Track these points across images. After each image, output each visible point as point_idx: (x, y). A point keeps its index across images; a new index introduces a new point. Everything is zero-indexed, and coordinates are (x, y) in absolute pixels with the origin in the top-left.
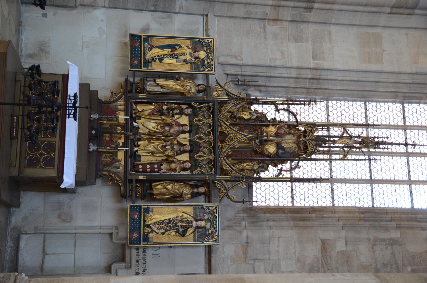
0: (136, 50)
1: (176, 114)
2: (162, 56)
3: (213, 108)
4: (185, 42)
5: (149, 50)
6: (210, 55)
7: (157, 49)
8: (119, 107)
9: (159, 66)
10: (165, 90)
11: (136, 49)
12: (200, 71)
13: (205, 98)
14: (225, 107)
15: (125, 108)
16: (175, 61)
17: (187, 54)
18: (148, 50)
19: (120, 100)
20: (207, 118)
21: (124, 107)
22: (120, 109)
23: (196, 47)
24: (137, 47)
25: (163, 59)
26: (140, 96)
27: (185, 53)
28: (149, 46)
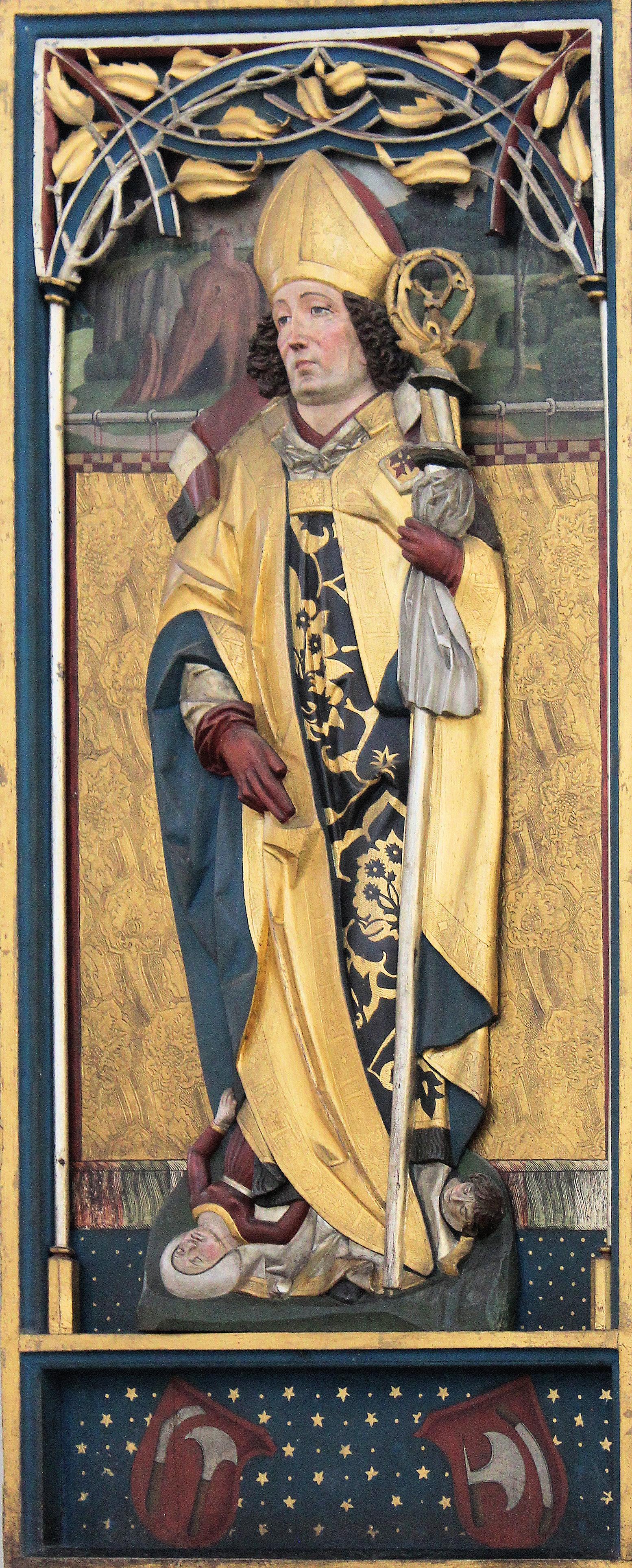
4: (115, 569)
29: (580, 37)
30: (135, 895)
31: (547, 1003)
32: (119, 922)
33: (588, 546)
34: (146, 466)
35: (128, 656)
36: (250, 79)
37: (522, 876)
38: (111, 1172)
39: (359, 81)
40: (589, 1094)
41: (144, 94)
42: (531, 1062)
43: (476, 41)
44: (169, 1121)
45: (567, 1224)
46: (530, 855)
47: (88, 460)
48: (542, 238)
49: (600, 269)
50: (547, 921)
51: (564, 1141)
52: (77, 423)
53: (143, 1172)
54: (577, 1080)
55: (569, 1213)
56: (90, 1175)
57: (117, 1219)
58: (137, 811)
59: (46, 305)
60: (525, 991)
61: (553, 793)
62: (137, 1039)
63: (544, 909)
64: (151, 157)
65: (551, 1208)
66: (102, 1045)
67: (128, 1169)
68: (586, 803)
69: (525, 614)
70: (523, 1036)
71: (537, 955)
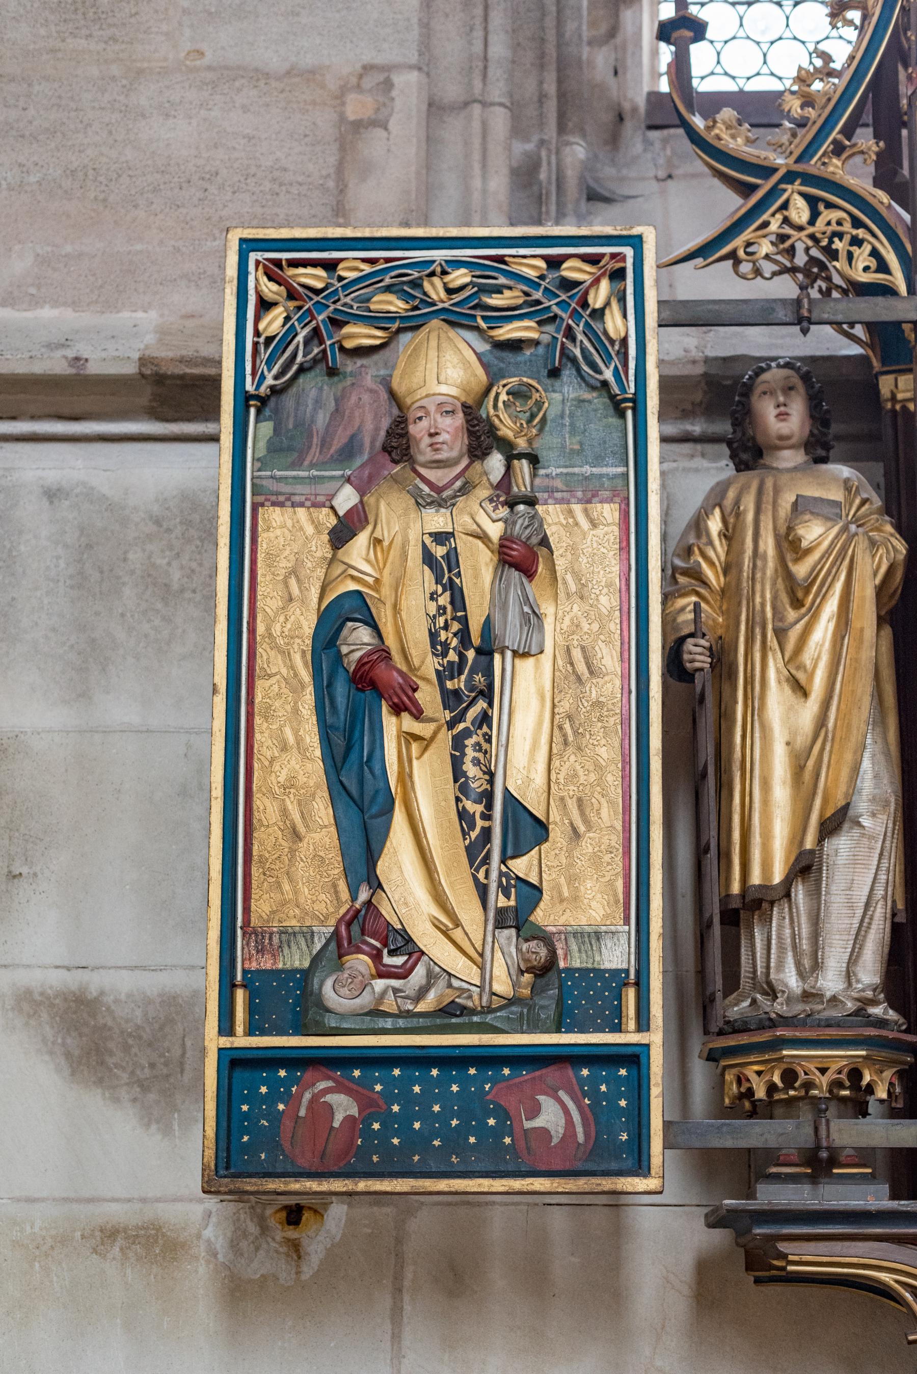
0: (406, 1118)
2: (471, 807)
4: (284, 564)
5: (399, 960)
6: (435, 290)
7: (382, 867)
9: (587, 846)
10: (867, 784)
11: (387, 1119)
12: (638, 403)
16: (526, 667)
17: (441, 538)
18: (404, 973)
23: (339, 440)
24: (367, 1104)
27: (428, 559)
28: (361, 962)
30: (293, 762)
31: (582, 828)
32: (282, 779)
33: (612, 553)
34: (308, 503)
35: (293, 617)
36: (392, 278)
37: (565, 751)
38: (271, 934)
39: (467, 279)
40: (612, 885)
41: (319, 285)
42: (571, 865)
44: (314, 902)
45: (596, 966)
46: (571, 738)
47: (267, 500)
49: (632, 390)
50: (582, 779)
51: (594, 914)
52: (259, 477)
53: (295, 934)
55: (597, 958)
56: (257, 935)
57: (275, 963)
58: (296, 711)
59: (248, 407)
60: (566, 822)
61: (588, 701)
62: (292, 851)
63: (581, 772)
64: (323, 321)
65: (584, 955)
66: (267, 855)
67: (283, 932)
68: (610, 706)
69: (568, 594)
70: (565, 849)
71: (575, 799)
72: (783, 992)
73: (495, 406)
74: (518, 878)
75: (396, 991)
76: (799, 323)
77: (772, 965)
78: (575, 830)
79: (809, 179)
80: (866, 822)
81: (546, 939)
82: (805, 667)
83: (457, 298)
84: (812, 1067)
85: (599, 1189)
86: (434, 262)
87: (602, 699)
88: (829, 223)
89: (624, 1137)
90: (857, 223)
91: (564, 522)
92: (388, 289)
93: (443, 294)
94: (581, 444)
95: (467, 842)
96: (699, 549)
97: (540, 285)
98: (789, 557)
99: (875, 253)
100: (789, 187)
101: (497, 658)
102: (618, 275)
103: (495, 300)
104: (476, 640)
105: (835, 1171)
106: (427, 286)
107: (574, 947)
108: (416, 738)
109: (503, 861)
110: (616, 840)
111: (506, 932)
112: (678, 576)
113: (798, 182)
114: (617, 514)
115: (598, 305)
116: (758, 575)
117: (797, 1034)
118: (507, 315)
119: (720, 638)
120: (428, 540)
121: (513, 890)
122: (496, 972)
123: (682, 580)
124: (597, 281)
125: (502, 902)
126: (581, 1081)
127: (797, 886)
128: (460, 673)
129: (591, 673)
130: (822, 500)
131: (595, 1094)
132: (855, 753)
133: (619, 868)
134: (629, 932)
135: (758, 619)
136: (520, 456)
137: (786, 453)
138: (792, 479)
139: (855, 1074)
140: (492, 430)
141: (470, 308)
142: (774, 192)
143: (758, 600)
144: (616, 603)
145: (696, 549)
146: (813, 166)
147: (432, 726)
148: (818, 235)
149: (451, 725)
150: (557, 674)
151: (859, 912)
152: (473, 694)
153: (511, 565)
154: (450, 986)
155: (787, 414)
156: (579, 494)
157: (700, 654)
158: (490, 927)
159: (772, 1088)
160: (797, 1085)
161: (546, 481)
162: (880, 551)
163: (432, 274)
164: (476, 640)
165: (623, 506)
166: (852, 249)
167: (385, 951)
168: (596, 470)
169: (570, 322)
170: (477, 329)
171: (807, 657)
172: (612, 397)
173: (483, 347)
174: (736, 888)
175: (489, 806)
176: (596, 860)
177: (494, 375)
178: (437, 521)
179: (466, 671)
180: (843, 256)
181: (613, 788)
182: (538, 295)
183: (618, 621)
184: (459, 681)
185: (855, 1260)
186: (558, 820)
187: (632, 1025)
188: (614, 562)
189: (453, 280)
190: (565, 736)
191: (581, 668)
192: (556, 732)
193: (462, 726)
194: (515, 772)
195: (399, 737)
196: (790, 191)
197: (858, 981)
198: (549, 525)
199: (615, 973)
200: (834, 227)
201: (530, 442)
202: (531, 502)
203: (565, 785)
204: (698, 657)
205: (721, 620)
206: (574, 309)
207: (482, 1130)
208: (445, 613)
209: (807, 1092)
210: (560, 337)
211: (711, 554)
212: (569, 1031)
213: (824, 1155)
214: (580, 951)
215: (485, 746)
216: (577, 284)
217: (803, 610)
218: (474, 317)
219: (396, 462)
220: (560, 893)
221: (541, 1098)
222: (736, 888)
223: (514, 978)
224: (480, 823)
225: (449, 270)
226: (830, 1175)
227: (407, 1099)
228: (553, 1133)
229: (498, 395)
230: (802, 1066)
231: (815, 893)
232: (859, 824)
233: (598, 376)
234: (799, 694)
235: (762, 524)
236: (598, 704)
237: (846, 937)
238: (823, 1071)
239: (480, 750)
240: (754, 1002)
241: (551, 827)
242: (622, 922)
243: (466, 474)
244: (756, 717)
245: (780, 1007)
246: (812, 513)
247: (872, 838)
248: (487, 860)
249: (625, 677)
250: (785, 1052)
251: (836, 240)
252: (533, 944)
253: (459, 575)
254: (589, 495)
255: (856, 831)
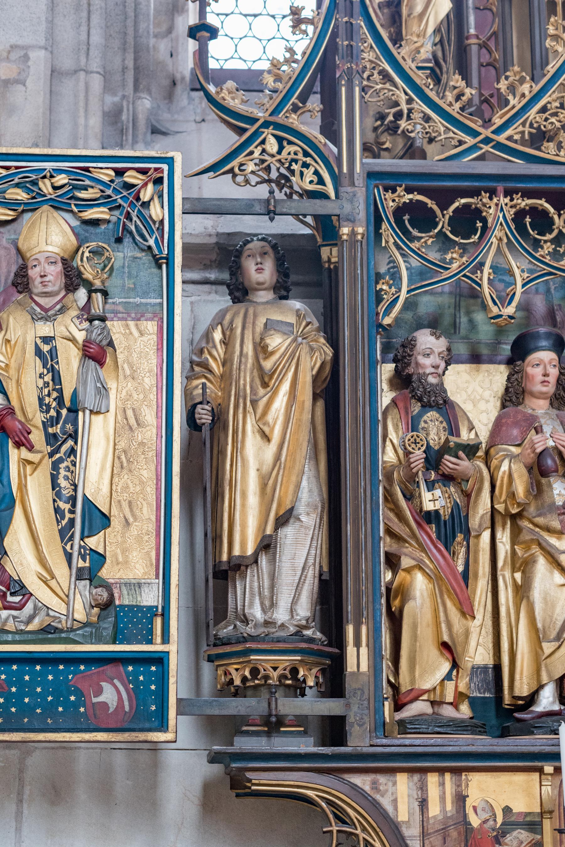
1: (453, 430)
3: (409, 190)
5: (17, 599)
6: (46, 187)
8: (434, 810)
9: (134, 530)
10: (304, 495)
13: (353, 233)
14: (398, 115)
15: (441, 771)
16: (98, 420)
17: (47, 340)
18: (20, 607)
19: (389, 809)
20: (485, 228)
21: (432, 779)
22: (449, 807)
25: (86, 499)
26: (364, 667)
27: (39, 352)
29: (162, 171)
31: (131, 520)
39: (66, 181)
40: (149, 554)
42: (124, 542)
43: (115, 170)
45: (138, 604)
46: (125, 464)
48: (141, 240)
49: (166, 252)
51: (137, 572)
54: (144, 549)
55: (139, 599)
60: (122, 515)
63: (131, 485)
65: (131, 597)
68: (150, 445)
71: (127, 502)
72: (252, 621)
73: (82, 260)
74: (91, 549)
75: (14, 617)
76: (268, 214)
77: (246, 604)
78: (126, 520)
79: (278, 126)
80: (303, 518)
81: (108, 587)
82: (269, 424)
83: (60, 192)
84: (268, 666)
85: (137, 739)
86: (46, 169)
87: (145, 441)
88: (289, 154)
89: (153, 708)
90: (306, 154)
91: (123, 332)
92: (17, 185)
93: (51, 190)
94: (135, 284)
95: (60, 527)
96: (208, 350)
97: (111, 186)
98: (261, 356)
99: (316, 173)
100: (266, 130)
101: (81, 414)
102: (159, 181)
103: (82, 195)
104: (68, 403)
105: (282, 729)
106: (41, 184)
107: (125, 592)
108: (30, 462)
109: (82, 539)
110: (152, 527)
111: (83, 582)
112: (194, 366)
113: (271, 127)
114: (156, 328)
115: (146, 199)
116: (243, 367)
117: (259, 646)
118: (91, 203)
119: (220, 405)
120: (39, 341)
121: (88, 557)
122: (76, 606)
123: (197, 369)
124: (146, 184)
125: (81, 564)
126: (128, 674)
127: (262, 556)
128: (57, 423)
129: (138, 424)
130: (282, 322)
131: (136, 682)
132: (298, 476)
133: (153, 544)
134: (159, 583)
135: (241, 394)
136: (96, 291)
137: (262, 293)
138: (265, 309)
139: (294, 671)
140: (80, 274)
141: (68, 199)
142: (256, 134)
143: (242, 382)
144: (154, 382)
145: (206, 350)
146: (280, 118)
147: (39, 456)
148: (283, 161)
149: (51, 455)
150: (117, 425)
151: (299, 573)
152: (65, 437)
153: (90, 358)
154: (48, 615)
155: (262, 269)
156: (133, 315)
157: (205, 414)
158: (73, 579)
159: (244, 679)
160: (259, 677)
161: (113, 307)
162: (316, 354)
163: (44, 177)
164: (68, 403)
165: (160, 323)
166: (303, 169)
167: (8, 593)
168: (143, 301)
169: (129, 209)
170: (72, 211)
171: (270, 418)
172: (154, 256)
173: (75, 223)
174: (225, 557)
175: (74, 505)
176: (139, 539)
177: (81, 241)
178: (45, 329)
179: (61, 422)
180: (297, 173)
181: (150, 495)
182: (109, 192)
183: (155, 393)
184: (57, 428)
185: (292, 783)
186: (116, 514)
187: (159, 640)
188: (153, 357)
189: (57, 181)
190: (121, 463)
191: (132, 421)
192: (116, 460)
193: (58, 456)
194: (90, 484)
195: (19, 462)
196: (266, 133)
197: (297, 615)
198: (114, 333)
199: (150, 608)
200: (292, 156)
201: (103, 282)
202: (103, 319)
203: (122, 493)
204: (204, 416)
205: (220, 394)
206: (131, 201)
207: (67, 704)
208: (48, 386)
209: (266, 682)
210: (122, 218)
211: (215, 353)
212: (121, 643)
213: (274, 719)
214: (128, 594)
215: (72, 468)
216: (134, 186)
217: (269, 389)
218: (70, 204)
219: (20, 292)
220: (117, 559)
221: (103, 684)
222: (225, 557)
223: (88, 610)
224: (68, 516)
225: (55, 175)
226: (279, 732)
227: (21, 684)
228: (110, 705)
229: (83, 253)
230: (262, 666)
231: (273, 561)
232: (299, 519)
233: (145, 243)
234: (265, 440)
235: (246, 336)
236: (142, 444)
237: (291, 588)
238: (275, 669)
239: (69, 471)
240: (235, 626)
241: (112, 519)
242: (154, 577)
243: (63, 301)
244: (239, 454)
245: (250, 630)
246: (275, 330)
247: (307, 528)
248: (72, 538)
249: (159, 428)
250: (252, 657)
251: (293, 164)
252: (99, 590)
253: (57, 363)
254: (139, 316)
255: (298, 524)
